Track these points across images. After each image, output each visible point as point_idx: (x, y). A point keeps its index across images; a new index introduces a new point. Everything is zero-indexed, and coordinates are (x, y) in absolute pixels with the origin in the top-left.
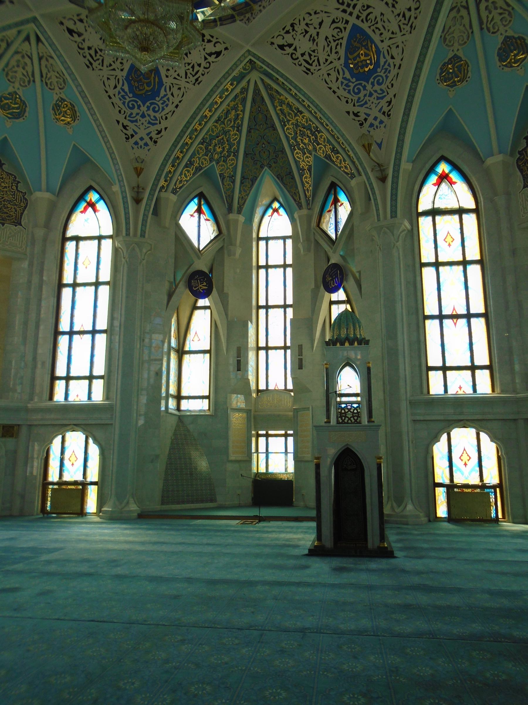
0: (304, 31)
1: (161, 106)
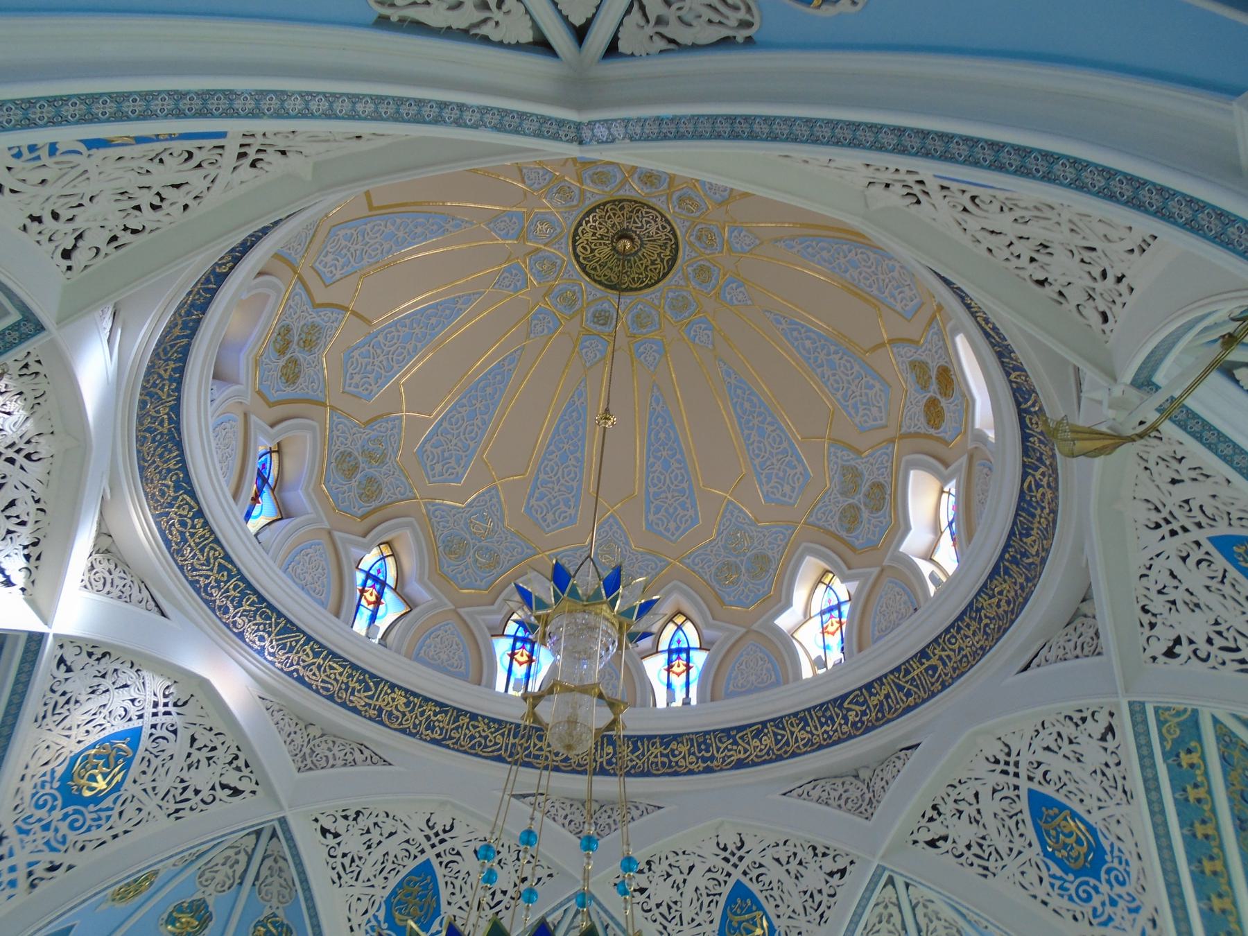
0: (1169, 605)
1: (1121, 868)
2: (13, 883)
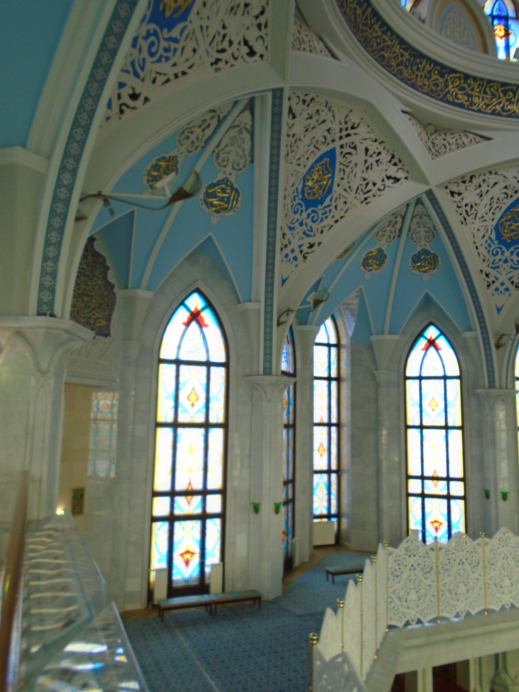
2: (295, 258)
